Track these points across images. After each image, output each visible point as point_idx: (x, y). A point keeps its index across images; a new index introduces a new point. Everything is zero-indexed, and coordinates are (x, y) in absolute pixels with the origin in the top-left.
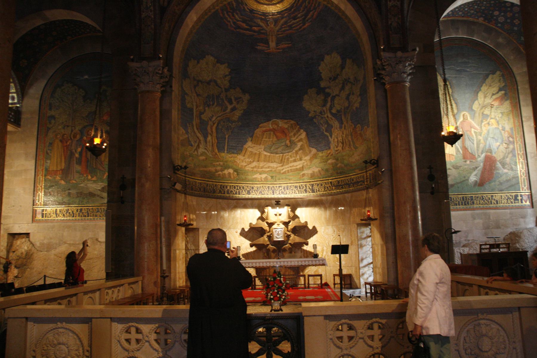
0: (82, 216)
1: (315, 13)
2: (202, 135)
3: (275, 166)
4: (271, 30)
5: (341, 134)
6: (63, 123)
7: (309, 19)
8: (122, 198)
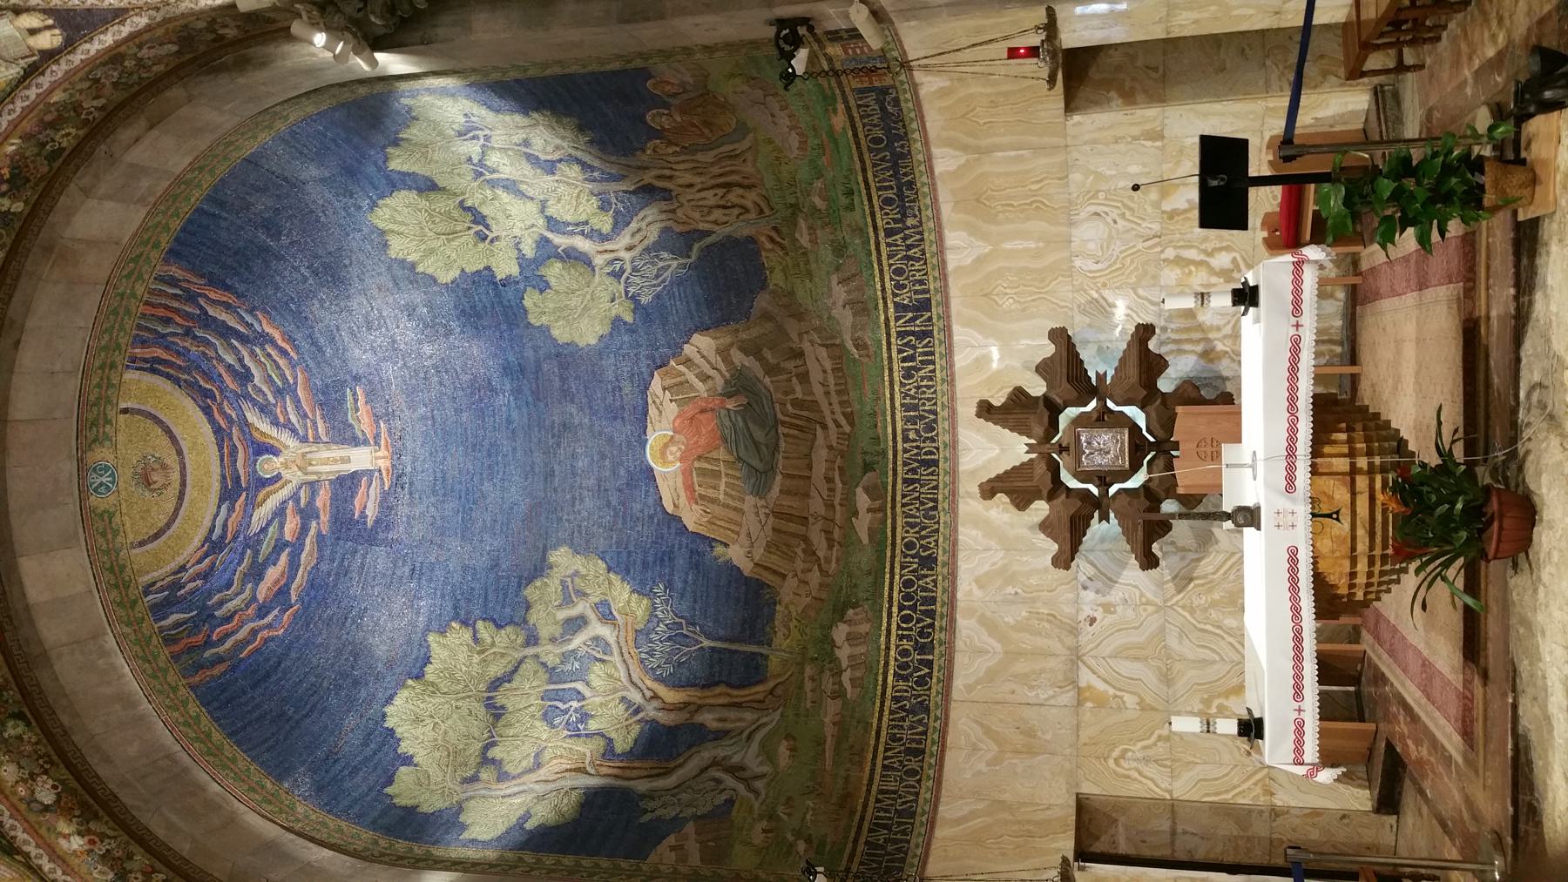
1: (212, 296)
2: (694, 749)
3: (824, 453)
4: (300, 469)
5: (690, 194)
7: (242, 318)
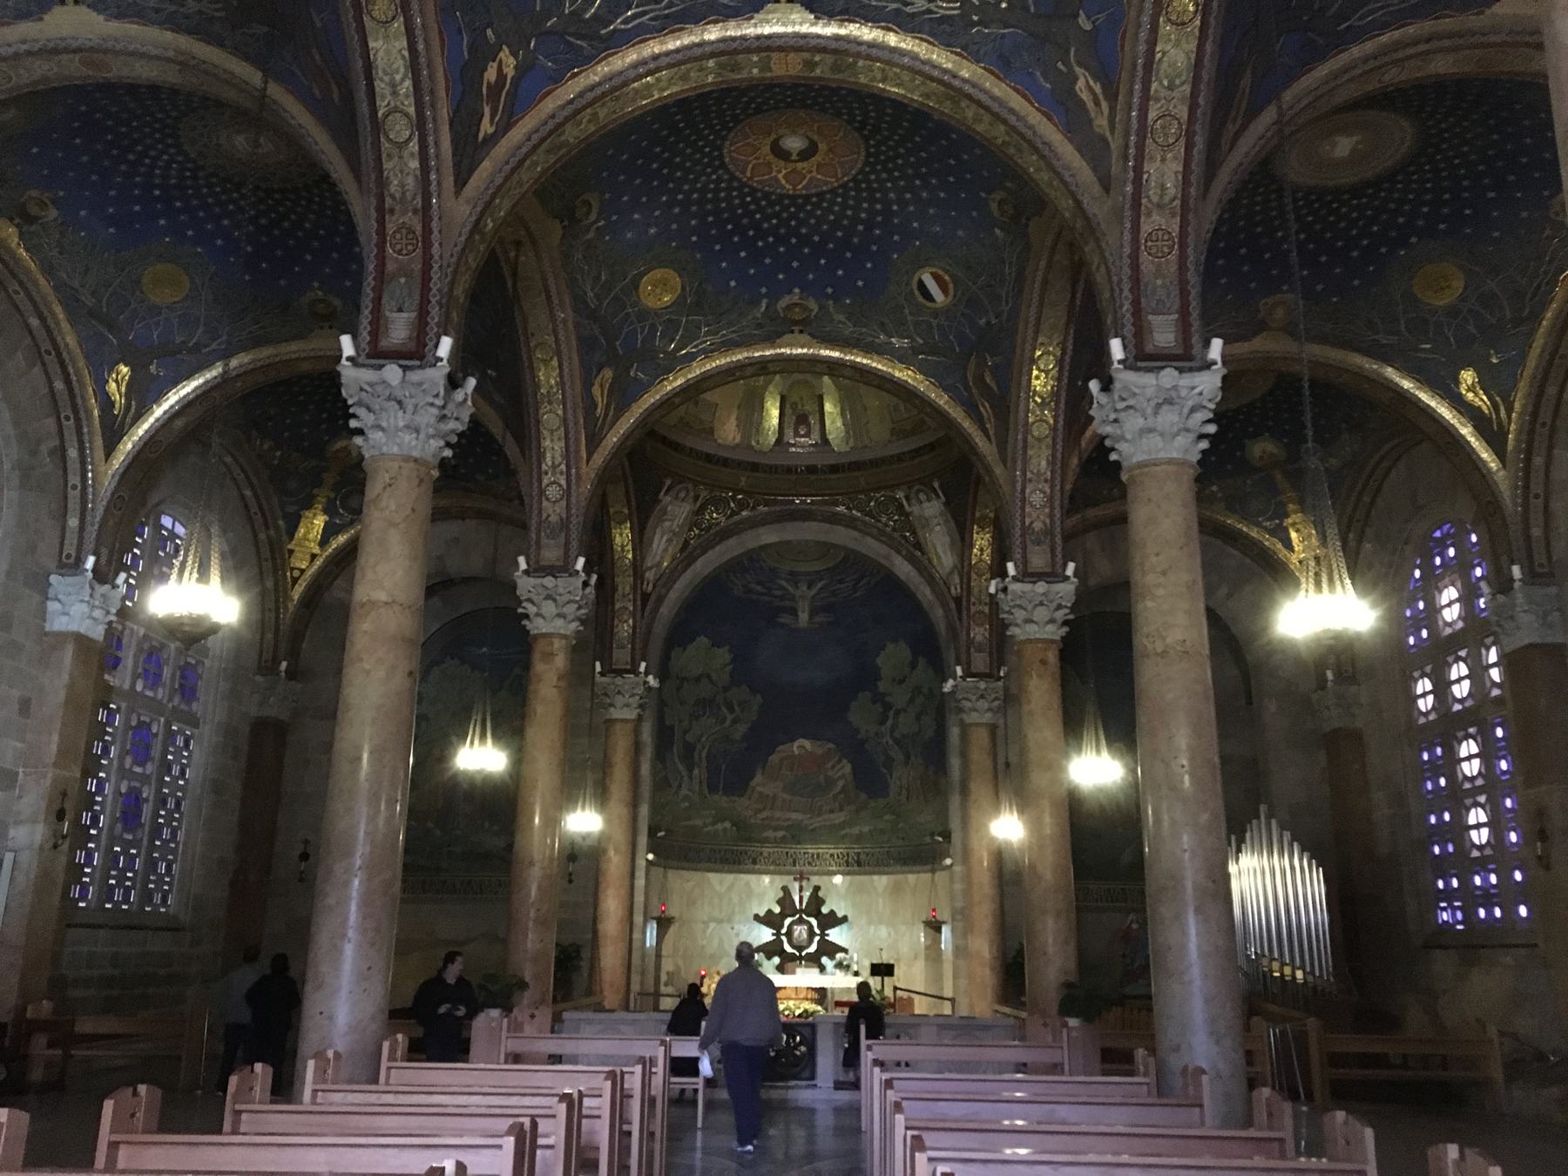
8: (570, 874)
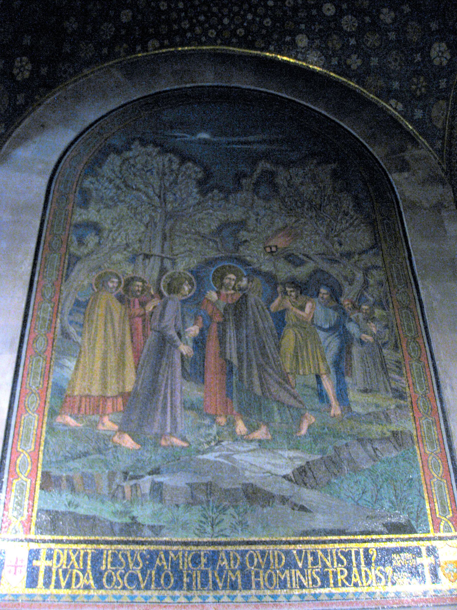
0: (220, 585)
6: (128, 245)
